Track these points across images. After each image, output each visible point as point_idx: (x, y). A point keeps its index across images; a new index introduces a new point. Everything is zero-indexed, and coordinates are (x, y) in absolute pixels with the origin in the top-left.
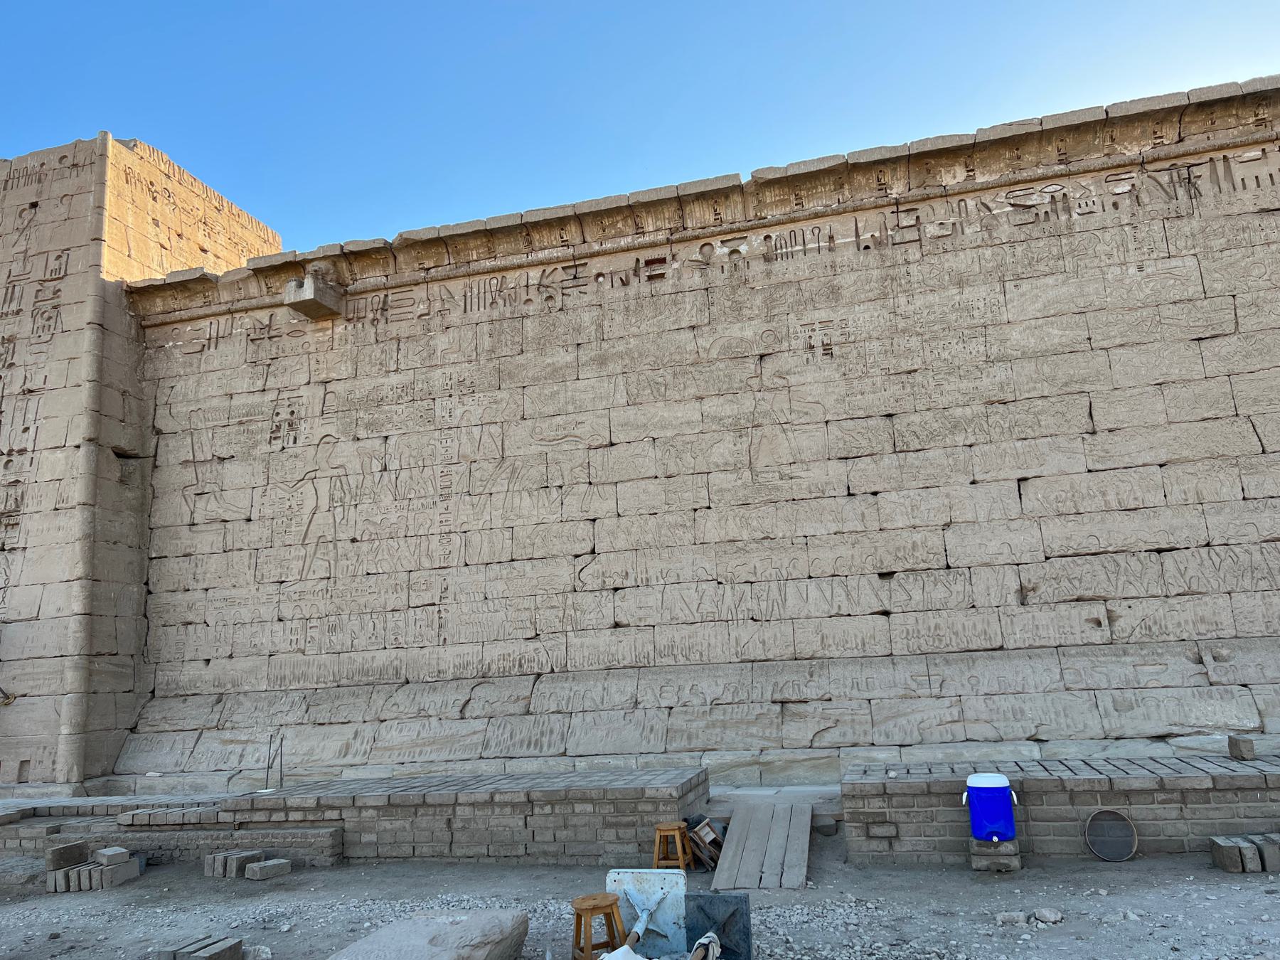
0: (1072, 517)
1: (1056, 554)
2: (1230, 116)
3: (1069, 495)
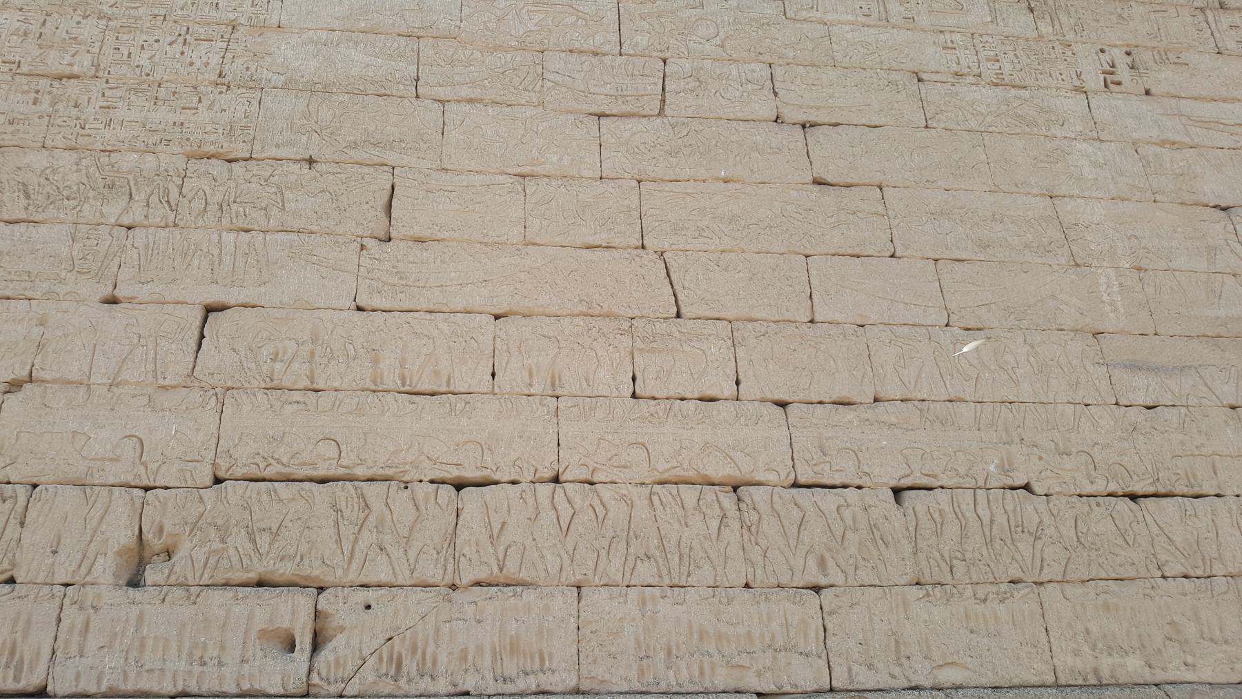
0: (296, 396)
1: (239, 472)
3: (305, 350)
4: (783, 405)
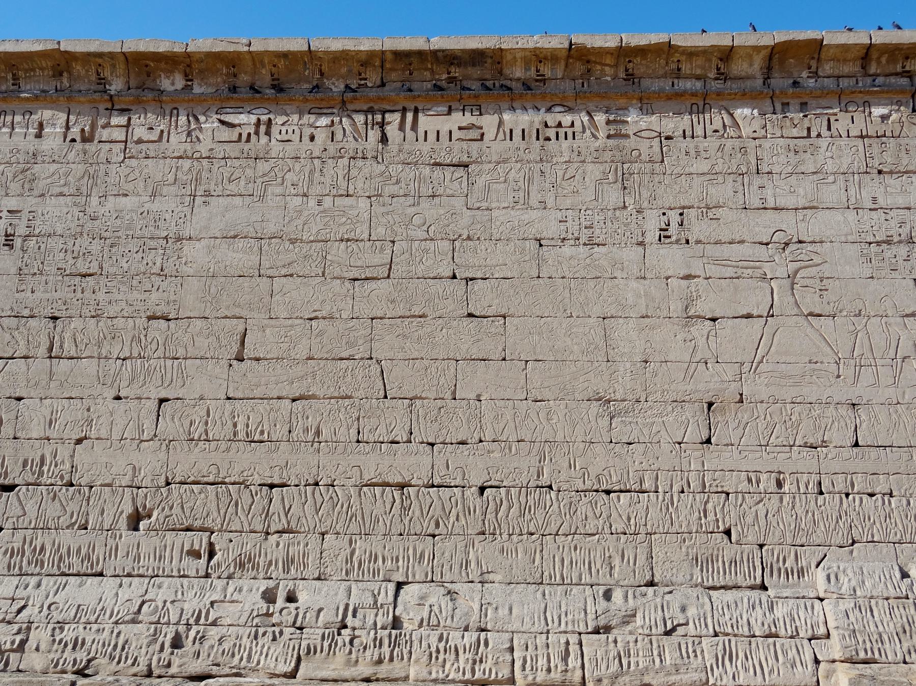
2: (426, 69)
4: (432, 445)
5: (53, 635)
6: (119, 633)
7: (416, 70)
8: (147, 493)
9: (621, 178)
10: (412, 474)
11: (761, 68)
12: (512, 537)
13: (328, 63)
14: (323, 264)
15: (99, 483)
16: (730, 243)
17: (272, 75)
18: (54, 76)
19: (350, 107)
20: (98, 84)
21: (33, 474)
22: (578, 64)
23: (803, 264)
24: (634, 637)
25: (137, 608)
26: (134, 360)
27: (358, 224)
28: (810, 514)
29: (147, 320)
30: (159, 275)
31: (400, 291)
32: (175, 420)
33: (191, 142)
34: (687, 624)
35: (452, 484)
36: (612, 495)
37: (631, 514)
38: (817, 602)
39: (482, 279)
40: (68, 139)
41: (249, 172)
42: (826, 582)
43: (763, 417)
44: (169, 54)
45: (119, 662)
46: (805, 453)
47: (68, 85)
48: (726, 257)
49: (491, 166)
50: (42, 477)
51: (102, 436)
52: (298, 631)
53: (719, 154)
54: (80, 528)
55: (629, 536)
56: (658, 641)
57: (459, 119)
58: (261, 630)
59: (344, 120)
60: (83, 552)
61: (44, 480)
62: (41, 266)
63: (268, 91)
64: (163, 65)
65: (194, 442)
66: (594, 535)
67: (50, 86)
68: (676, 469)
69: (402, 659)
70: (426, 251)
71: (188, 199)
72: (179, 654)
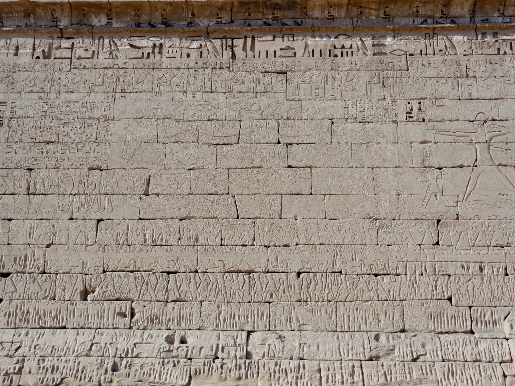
2: (259, 12)
4: (267, 247)
5: (39, 364)
6: (79, 363)
7: (253, 12)
8: (92, 278)
9: (382, 81)
10: (256, 265)
11: (469, 11)
12: (318, 303)
13: (198, 8)
14: (197, 135)
15: (61, 272)
16: (450, 121)
17: (162, 16)
18: (24, 17)
19: (212, 36)
20: (53, 21)
21: (21, 266)
22: (355, 9)
23: (495, 134)
24: (394, 363)
25: (89, 347)
26: (81, 196)
27: (219, 110)
28: (500, 288)
29: (88, 171)
30: (95, 142)
31: (245, 152)
32: (108, 232)
33: (112, 58)
34: (426, 354)
35: (280, 271)
36: (378, 277)
37: (390, 288)
38: (505, 341)
39: (296, 144)
40: (35, 56)
41: (149, 77)
42: (510, 328)
43: (471, 228)
44: (98, 3)
45: (80, 380)
46: (497, 251)
47: (34, 22)
48: (448, 130)
49: (301, 73)
50: (26, 268)
51: (62, 243)
52: (189, 361)
53: (443, 65)
54: (51, 299)
55: (390, 302)
56: (408, 364)
57: (280, 42)
58: (166, 361)
59: (208, 43)
60: (53, 314)
61: (27, 269)
62: (20, 137)
63: (160, 26)
64: (93, 10)
65: (120, 246)
66: (368, 301)
67: (22, 23)
68: (418, 260)
69: (253, 376)
70: (261, 126)
71: (111, 94)
72: (117, 375)
